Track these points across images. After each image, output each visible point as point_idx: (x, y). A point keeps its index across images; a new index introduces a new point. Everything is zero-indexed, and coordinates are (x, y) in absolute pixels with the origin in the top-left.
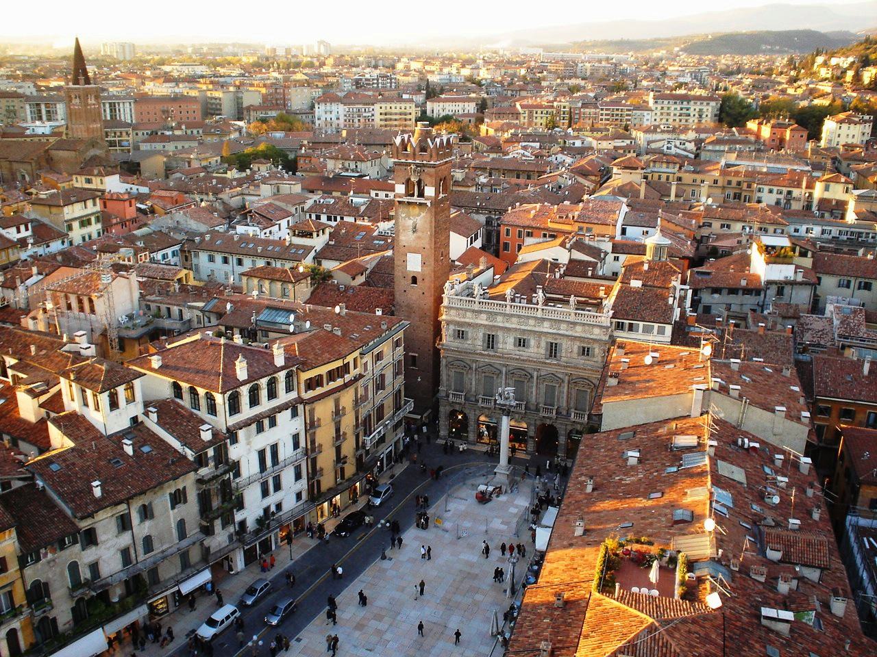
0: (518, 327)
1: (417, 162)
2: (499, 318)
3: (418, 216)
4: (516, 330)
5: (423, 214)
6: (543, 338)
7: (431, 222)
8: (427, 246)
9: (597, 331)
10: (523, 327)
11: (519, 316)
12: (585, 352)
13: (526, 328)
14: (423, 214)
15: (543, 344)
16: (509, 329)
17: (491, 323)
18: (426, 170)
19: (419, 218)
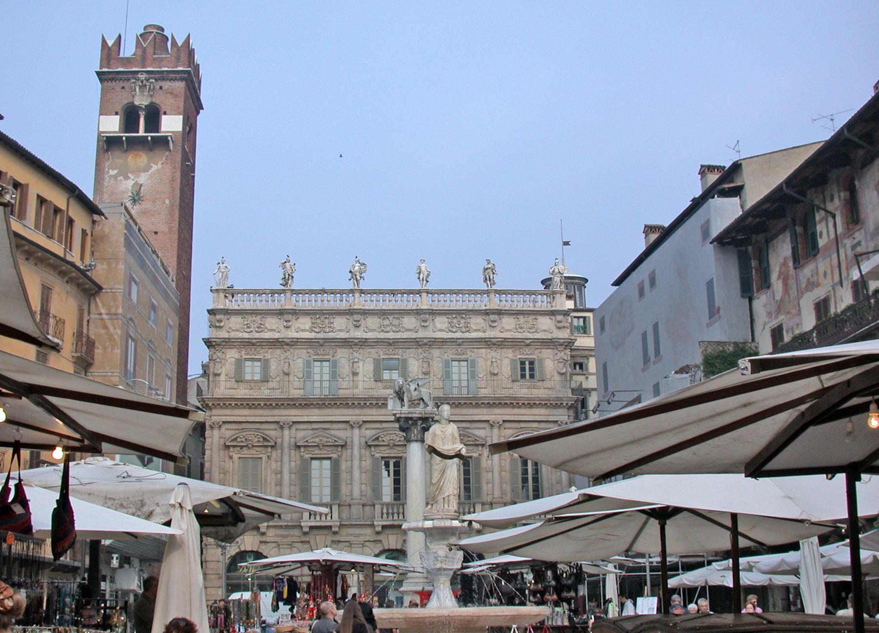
0: (382, 335)
1: (149, 69)
2: (340, 322)
3: (146, 170)
4: (378, 342)
5: (155, 167)
6: (436, 353)
7: (173, 180)
8: (162, 228)
9: (545, 323)
10: (391, 335)
11: (383, 313)
12: (527, 370)
13: (399, 335)
14: (155, 167)
15: (437, 367)
16: (363, 343)
17: (321, 336)
18: (166, 85)
19: (143, 178)
